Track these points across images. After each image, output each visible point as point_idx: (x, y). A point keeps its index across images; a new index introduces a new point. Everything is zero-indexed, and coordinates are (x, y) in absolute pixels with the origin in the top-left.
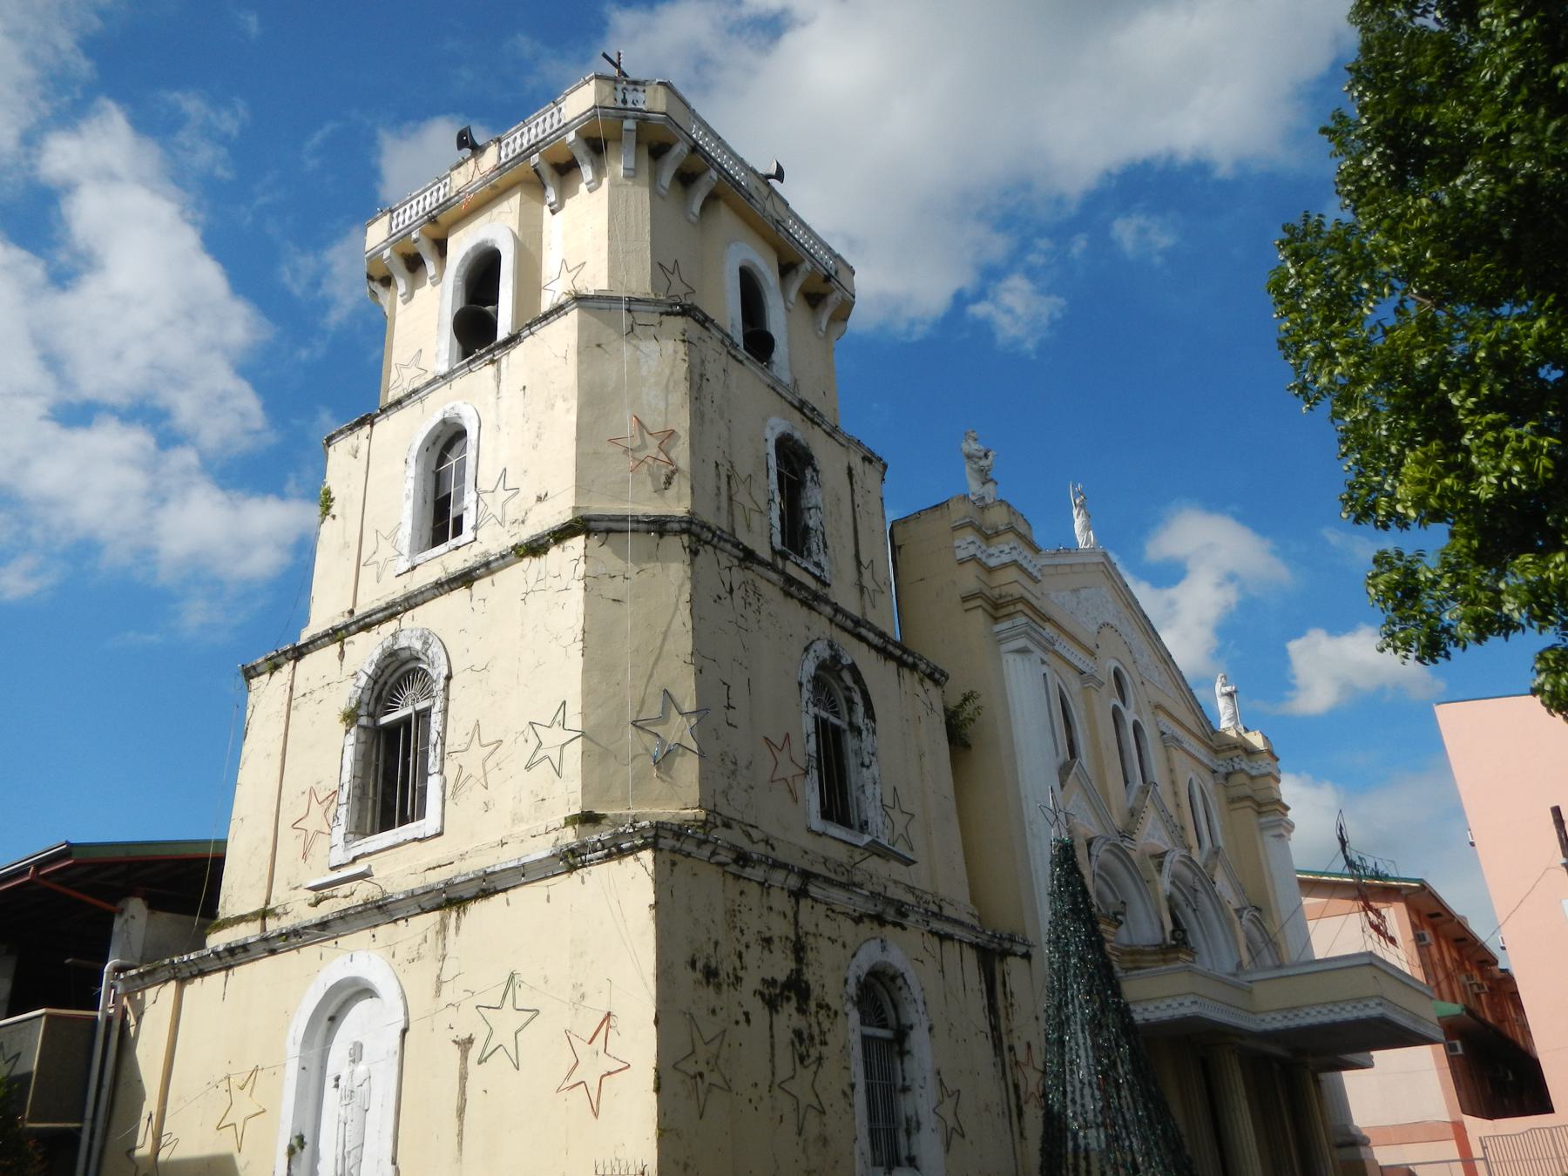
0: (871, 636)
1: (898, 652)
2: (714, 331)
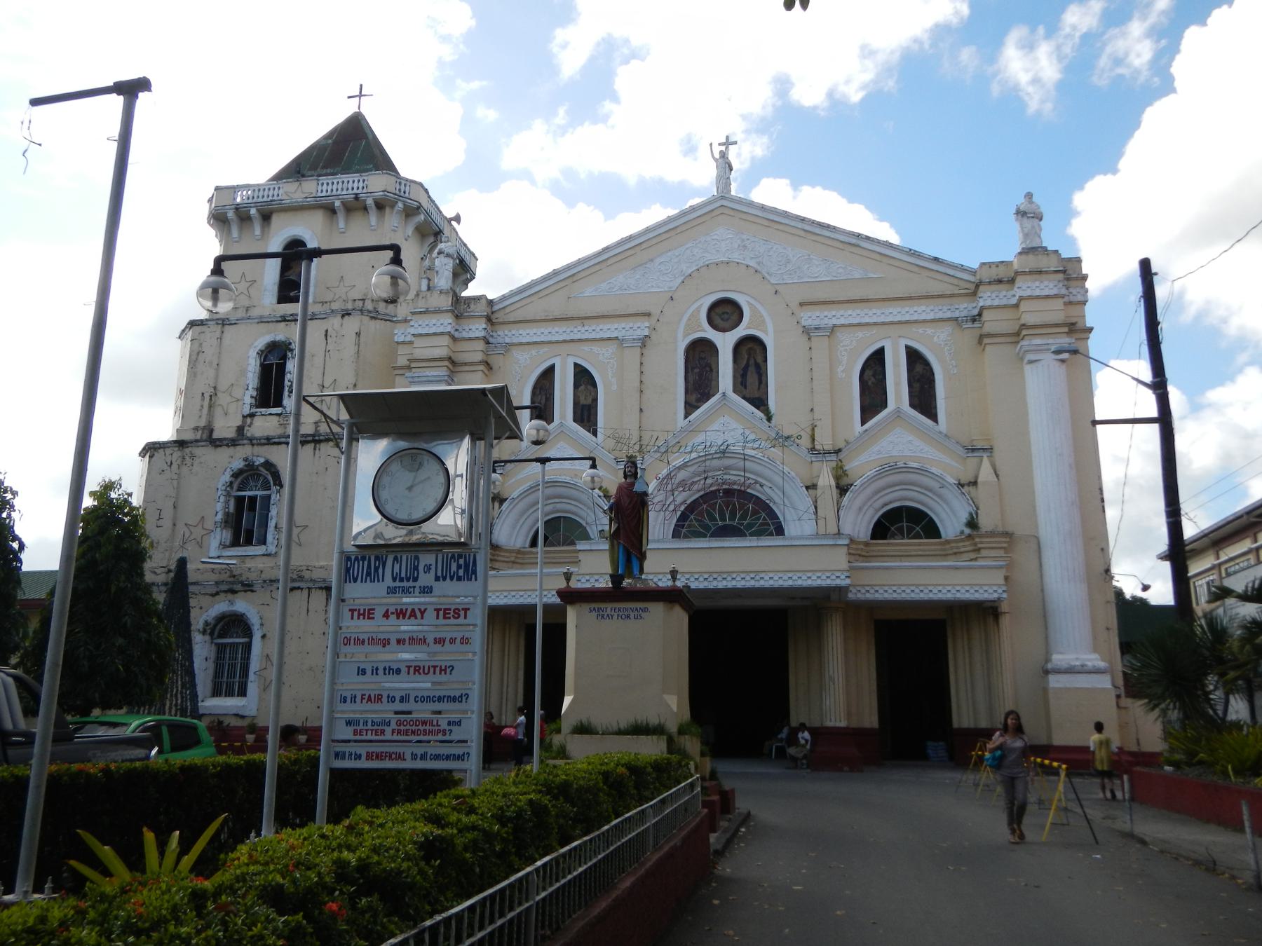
1: (310, 438)
2: (209, 323)
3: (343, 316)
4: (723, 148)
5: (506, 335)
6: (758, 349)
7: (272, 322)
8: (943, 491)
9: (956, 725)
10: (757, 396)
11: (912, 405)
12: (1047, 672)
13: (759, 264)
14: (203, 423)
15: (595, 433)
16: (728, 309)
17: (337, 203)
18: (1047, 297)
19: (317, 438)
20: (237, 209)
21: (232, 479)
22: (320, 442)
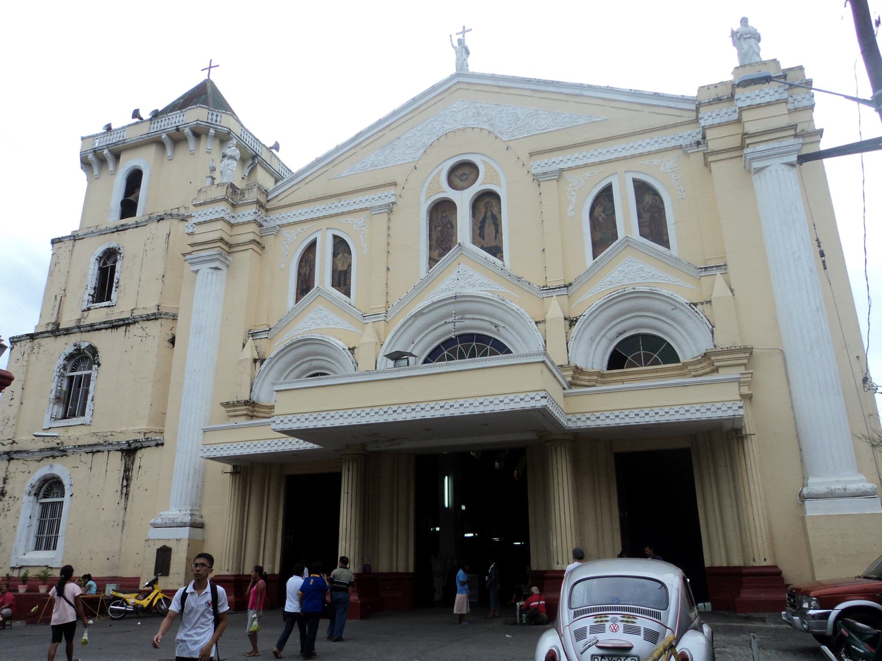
0: (103, 326)
1: (121, 323)
2: (64, 240)
3: (158, 221)
4: (460, 36)
5: (277, 218)
6: (494, 202)
7: (108, 233)
8: (676, 313)
9: (707, 564)
10: (494, 244)
11: (641, 235)
12: (803, 498)
13: (492, 125)
14: (53, 320)
15: (348, 294)
16: (466, 170)
17: (164, 136)
18: (769, 104)
19: (127, 322)
20: (95, 152)
21: (66, 362)
22: (128, 325)
